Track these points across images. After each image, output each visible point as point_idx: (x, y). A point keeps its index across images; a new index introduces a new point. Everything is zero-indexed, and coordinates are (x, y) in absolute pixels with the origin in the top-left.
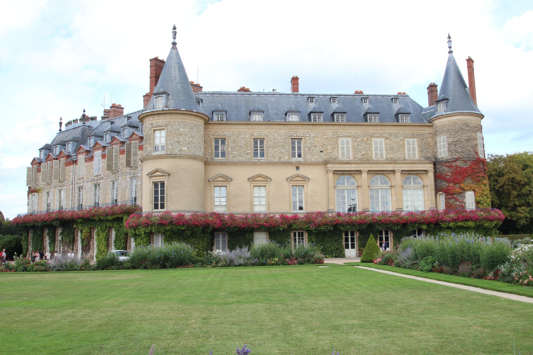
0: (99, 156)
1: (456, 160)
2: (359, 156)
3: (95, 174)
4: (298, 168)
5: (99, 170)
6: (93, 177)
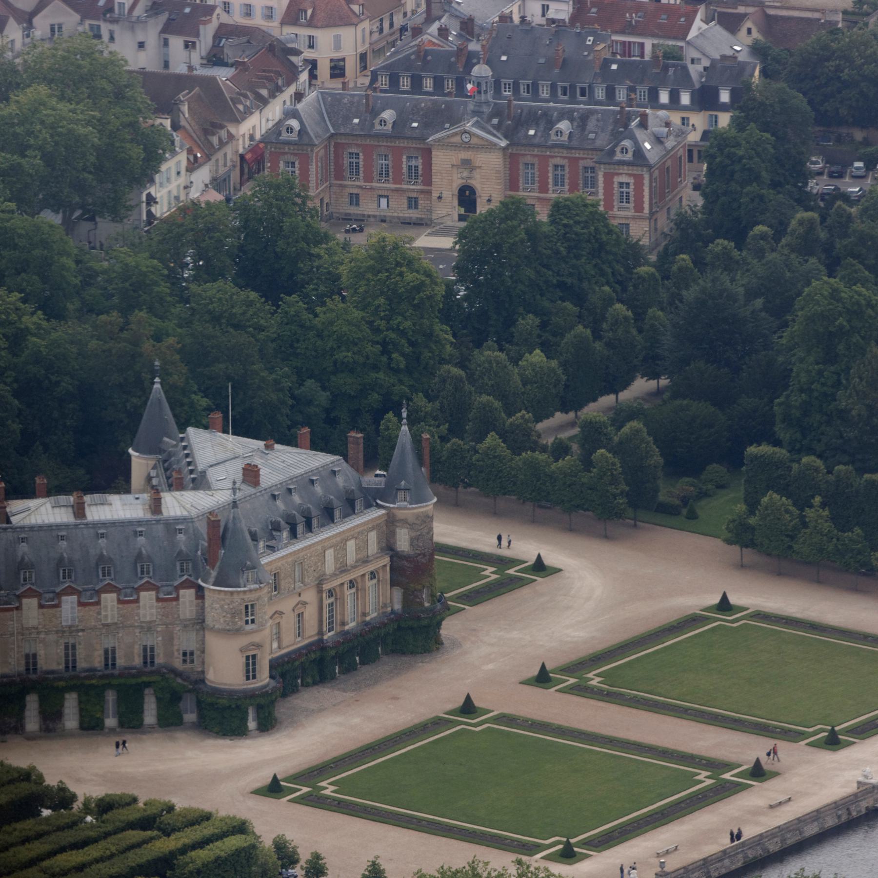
0: (72, 602)
1: (419, 555)
2: (338, 566)
3: (64, 624)
4: (300, 595)
5: (73, 619)
6: (60, 629)
